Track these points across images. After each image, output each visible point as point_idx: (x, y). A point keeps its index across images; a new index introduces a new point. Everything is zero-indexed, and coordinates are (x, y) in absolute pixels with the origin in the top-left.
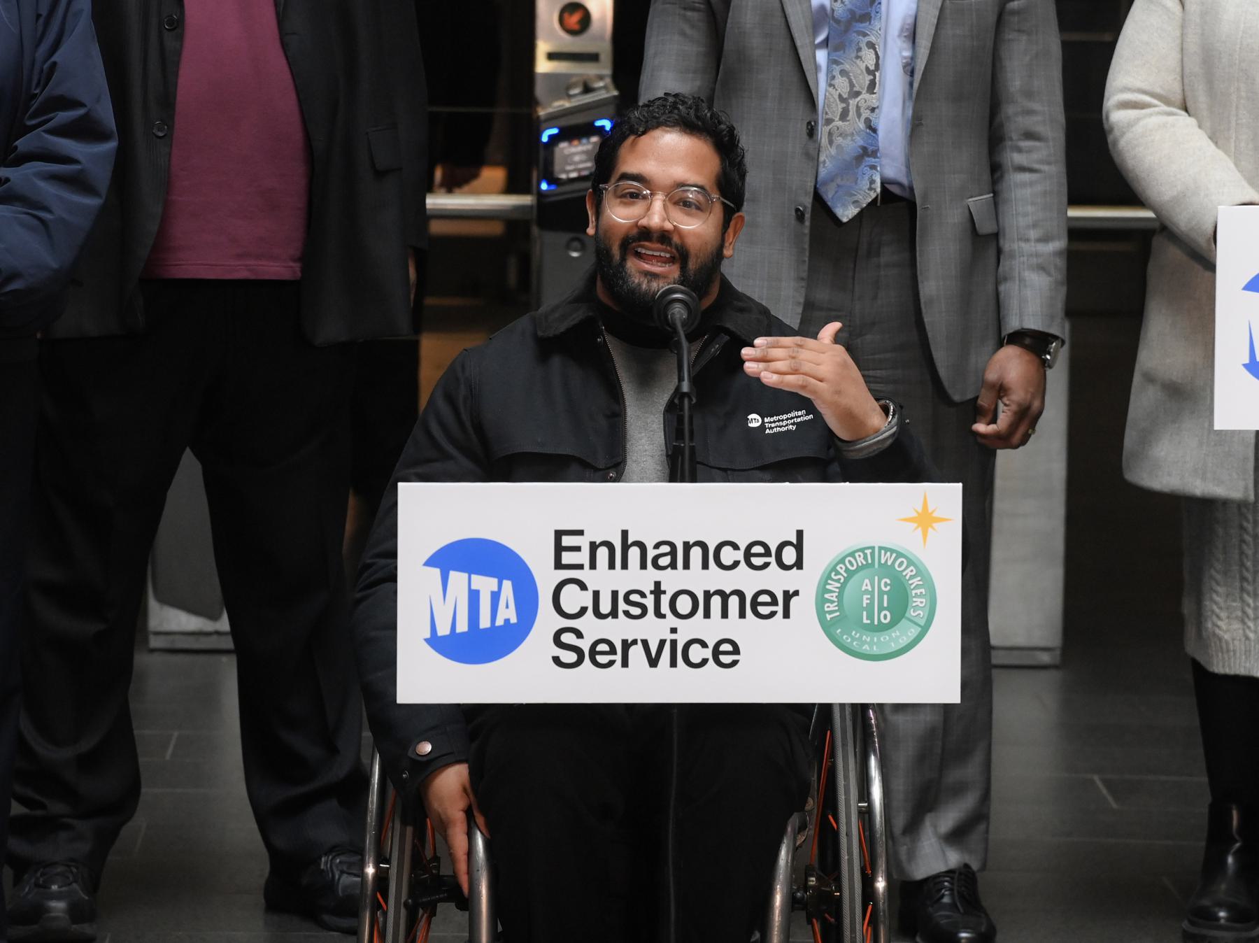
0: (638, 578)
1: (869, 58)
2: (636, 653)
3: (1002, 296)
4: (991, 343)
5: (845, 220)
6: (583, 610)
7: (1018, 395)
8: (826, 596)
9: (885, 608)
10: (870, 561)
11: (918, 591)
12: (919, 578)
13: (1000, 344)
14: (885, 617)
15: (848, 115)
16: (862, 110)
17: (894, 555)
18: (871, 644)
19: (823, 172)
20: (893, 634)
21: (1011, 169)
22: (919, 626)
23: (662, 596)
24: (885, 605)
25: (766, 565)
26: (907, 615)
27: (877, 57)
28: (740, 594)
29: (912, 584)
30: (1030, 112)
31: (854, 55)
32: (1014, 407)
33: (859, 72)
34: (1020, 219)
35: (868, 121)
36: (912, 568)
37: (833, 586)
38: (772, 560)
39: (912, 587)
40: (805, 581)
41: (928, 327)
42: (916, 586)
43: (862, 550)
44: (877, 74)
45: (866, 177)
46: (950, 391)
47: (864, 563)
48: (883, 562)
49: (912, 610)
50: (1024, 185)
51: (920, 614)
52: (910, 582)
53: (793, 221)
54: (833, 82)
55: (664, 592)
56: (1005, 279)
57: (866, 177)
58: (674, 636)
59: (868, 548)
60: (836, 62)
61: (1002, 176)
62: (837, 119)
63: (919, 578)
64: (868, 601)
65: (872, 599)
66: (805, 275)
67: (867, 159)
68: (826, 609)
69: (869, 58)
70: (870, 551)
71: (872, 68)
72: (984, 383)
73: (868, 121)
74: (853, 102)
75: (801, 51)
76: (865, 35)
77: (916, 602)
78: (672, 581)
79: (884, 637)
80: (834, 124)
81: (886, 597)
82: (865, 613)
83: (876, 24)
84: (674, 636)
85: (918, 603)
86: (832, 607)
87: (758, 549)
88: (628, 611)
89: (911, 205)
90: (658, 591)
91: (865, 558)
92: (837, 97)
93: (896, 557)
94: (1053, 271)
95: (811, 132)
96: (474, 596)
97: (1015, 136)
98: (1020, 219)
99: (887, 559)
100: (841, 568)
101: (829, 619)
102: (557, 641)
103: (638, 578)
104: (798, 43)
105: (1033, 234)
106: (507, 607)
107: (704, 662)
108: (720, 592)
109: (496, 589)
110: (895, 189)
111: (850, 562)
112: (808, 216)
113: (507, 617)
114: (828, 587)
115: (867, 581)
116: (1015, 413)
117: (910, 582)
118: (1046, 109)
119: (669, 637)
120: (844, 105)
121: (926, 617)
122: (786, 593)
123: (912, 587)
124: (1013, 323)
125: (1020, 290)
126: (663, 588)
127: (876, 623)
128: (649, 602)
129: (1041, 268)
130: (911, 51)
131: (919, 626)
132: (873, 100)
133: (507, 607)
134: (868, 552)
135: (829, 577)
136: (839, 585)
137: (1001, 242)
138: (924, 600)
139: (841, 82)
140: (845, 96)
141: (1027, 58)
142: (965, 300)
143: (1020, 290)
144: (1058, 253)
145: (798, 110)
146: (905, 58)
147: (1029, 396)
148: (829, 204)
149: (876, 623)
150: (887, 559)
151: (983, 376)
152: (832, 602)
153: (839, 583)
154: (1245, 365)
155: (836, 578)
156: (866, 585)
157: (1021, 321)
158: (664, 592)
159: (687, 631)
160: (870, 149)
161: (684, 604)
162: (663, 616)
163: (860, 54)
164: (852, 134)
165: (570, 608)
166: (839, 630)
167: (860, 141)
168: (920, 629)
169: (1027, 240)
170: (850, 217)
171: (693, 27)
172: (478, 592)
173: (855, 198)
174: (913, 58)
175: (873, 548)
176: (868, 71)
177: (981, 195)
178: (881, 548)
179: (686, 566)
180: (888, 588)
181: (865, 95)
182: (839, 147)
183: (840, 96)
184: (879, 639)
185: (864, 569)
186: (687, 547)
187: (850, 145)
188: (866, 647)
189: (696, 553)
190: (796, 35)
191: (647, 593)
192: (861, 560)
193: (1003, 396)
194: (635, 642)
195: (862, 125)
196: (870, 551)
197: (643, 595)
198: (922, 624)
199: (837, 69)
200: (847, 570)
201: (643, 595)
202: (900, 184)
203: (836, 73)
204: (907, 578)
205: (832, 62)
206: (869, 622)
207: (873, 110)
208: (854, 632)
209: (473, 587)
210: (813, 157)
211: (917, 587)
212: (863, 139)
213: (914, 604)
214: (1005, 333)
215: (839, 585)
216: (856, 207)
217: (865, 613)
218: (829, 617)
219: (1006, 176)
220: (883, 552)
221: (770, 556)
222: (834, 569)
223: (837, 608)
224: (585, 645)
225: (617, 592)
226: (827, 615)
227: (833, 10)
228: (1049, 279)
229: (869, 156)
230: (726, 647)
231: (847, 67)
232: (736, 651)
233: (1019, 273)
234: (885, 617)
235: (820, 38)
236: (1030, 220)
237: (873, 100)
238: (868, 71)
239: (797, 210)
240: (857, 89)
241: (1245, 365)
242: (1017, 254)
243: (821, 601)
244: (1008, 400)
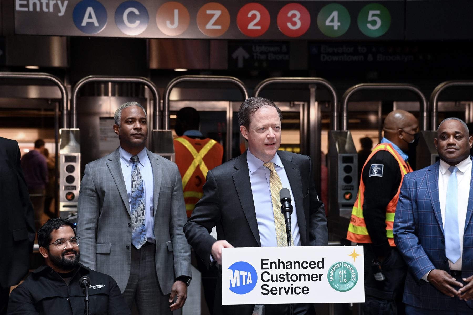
0: (282, 271)
1: (142, 207)
2: (283, 290)
3: (175, 267)
4: (173, 280)
5: (138, 249)
6: (269, 280)
7: (181, 294)
8: (330, 275)
11: (353, 274)
13: (175, 280)
15: (137, 222)
16: (141, 220)
17: (347, 264)
18: (342, 287)
19: (134, 235)
20: (347, 285)
21: (176, 235)
22: (354, 282)
24: (345, 277)
25: (315, 267)
26: (351, 280)
27: (144, 206)
28: (308, 275)
30: (179, 220)
31: (138, 206)
32: (180, 297)
33: (140, 210)
34: (179, 247)
35: (143, 223)
36: (351, 268)
37: (332, 272)
38: (316, 266)
39: (352, 272)
40: (325, 271)
41: (158, 276)
43: (339, 263)
44: (144, 211)
45: (143, 237)
46: (163, 292)
48: (344, 266)
50: (179, 238)
52: (351, 271)
53: (126, 249)
54: (133, 213)
55: (289, 275)
56: (176, 263)
57: (143, 237)
58: (292, 286)
59: (340, 263)
60: (134, 208)
61: (174, 237)
62: (135, 223)
66: (130, 263)
67: (143, 233)
68: (330, 279)
69: (142, 207)
71: (143, 209)
72: (172, 290)
73: (143, 223)
74: (138, 218)
75: (126, 205)
76: (141, 201)
78: (291, 272)
79: (345, 286)
80: (134, 224)
81: (345, 275)
82: (340, 279)
83: (143, 198)
84: (292, 286)
86: (332, 278)
87: (312, 263)
90: (287, 274)
91: (340, 265)
92: (134, 217)
94: (188, 260)
95: (130, 225)
96: (241, 277)
97: (176, 226)
98: (179, 247)
102: (262, 288)
103: (282, 271)
104: (125, 203)
105: (183, 251)
106: (250, 279)
107: (300, 293)
108: (303, 275)
109: (247, 275)
111: (336, 266)
112: (130, 247)
113: (250, 282)
114: (331, 273)
115: (340, 271)
116: (181, 298)
118: (184, 219)
119: (291, 286)
120: (136, 219)
121: (355, 280)
122: (320, 274)
124: (179, 274)
125: (180, 266)
126: (289, 274)
127: (343, 282)
128: (285, 277)
129: (185, 260)
130: (153, 204)
131: (354, 282)
133: (250, 279)
134: (340, 263)
136: (333, 272)
137: (174, 253)
138: (355, 276)
139: (135, 214)
140: (136, 217)
141: (178, 207)
142: (166, 268)
143: (180, 266)
144: (189, 256)
146: (151, 206)
147: (184, 294)
148: (134, 245)
149: (343, 282)
151: (172, 289)
152: (332, 277)
154: (229, 288)
155: (332, 270)
156: (340, 272)
157: (181, 273)
158: (289, 275)
159: (295, 284)
160: (144, 230)
161: (294, 278)
162: (289, 281)
163: (139, 206)
164: (139, 227)
166: (334, 284)
167: (141, 228)
168: (354, 283)
169: (181, 253)
170: (140, 248)
171: (93, 201)
173: (140, 243)
174: (154, 206)
175: (341, 263)
176: (142, 210)
177: (169, 241)
178: (343, 263)
179: (295, 268)
180: (346, 273)
181: (141, 216)
182: (136, 230)
183: (135, 217)
184: (344, 286)
186: (295, 263)
187: (139, 230)
188: (341, 288)
189: (297, 264)
190: (124, 201)
191: (285, 275)
192: (338, 266)
193: (177, 294)
194: (282, 288)
195: (141, 224)
197: (284, 276)
198: (355, 282)
199: (134, 210)
200: (335, 268)
201: (284, 276)
203: (134, 211)
204: (350, 270)
205: (133, 208)
206: (341, 282)
207: (144, 220)
208: (337, 285)
210: (130, 232)
212: (142, 228)
213: (352, 277)
214: (177, 277)
215: (333, 272)
216: (141, 245)
217: (340, 279)
218: (331, 280)
219: (175, 237)
220: (344, 264)
221: (316, 265)
222: (332, 268)
224: (269, 289)
225: (277, 275)
227: (132, 195)
228: (188, 262)
229: (143, 232)
230: (305, 289)
231: (136, 209)
232: (308, 290)
233: (180, 261)
235: (129, 201)
236: (182, 247)
237: (143, 217)
238: (142, 210)
239: (127, 246)
240: (139, 215)
241: (229, 288)
242: (179, 256)
243: (329, 277)
244: (179, 295)
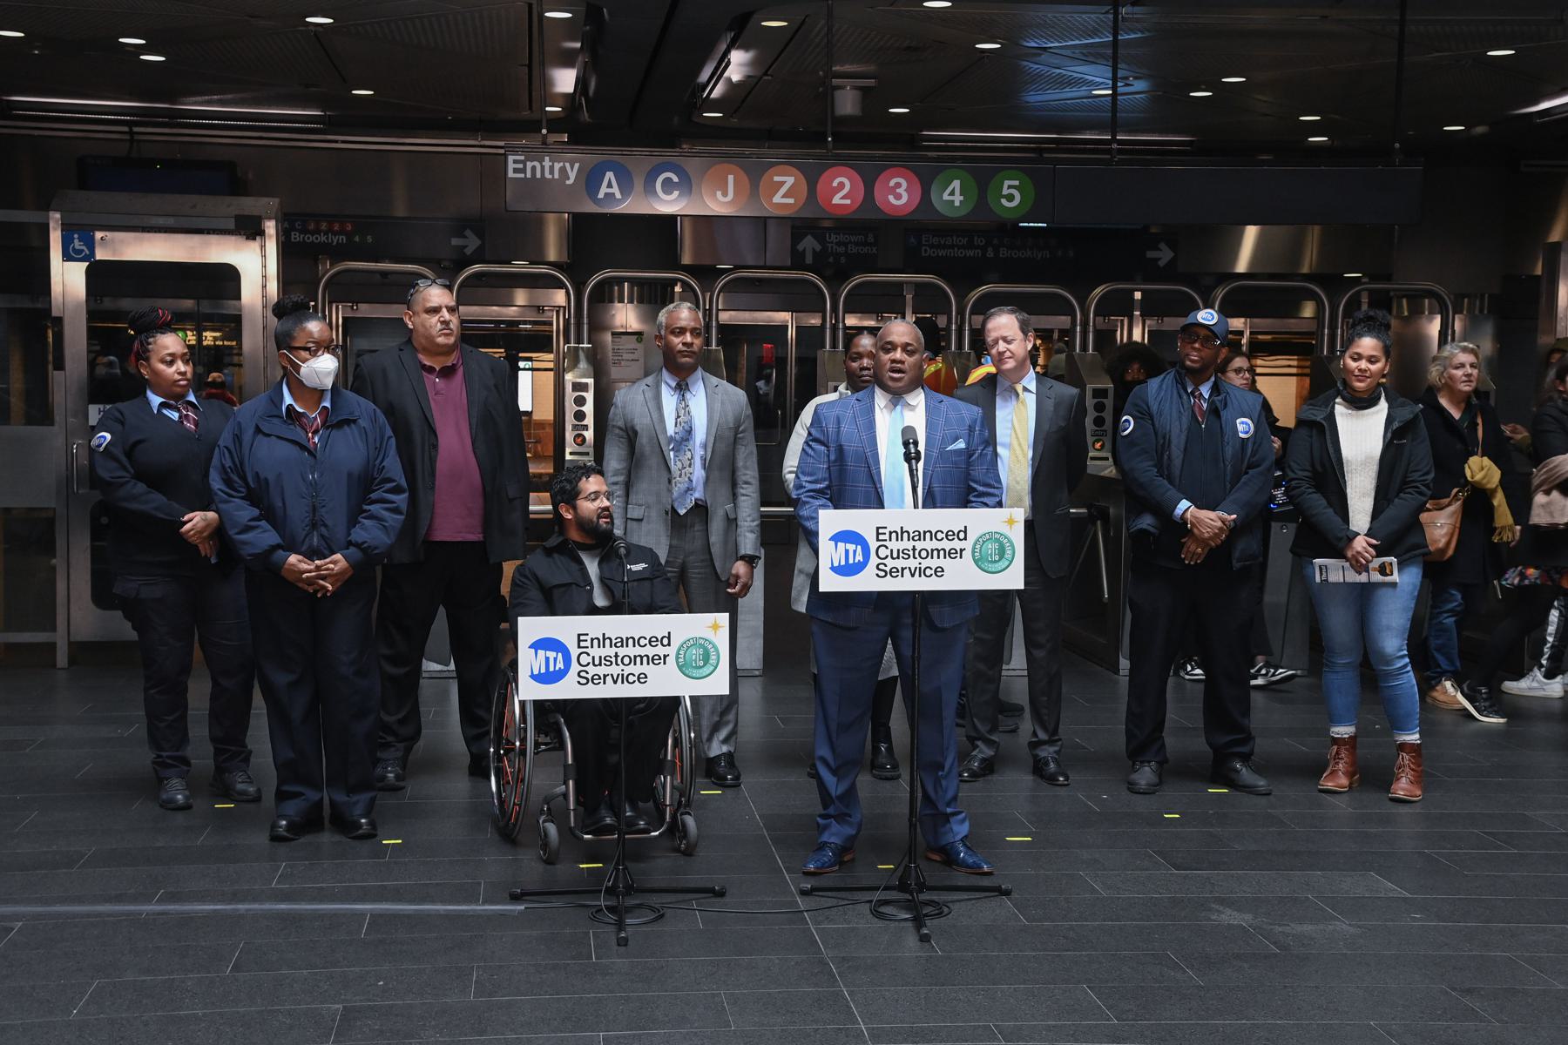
1: (689, 455)
19: (675, 494)
35: (689, 478)
69: (689, 455)
73: (689, 478)
89: (706, 508)
110: (700, 503)
132: (691, 470)
145: (665, 476)
187: (683, 487)
195: (687, 479)
199: (677, 459)
202: (701, 500)
210: (670, 491)
231: (680, 458)
235: (671, 447)
237: (691, 470)
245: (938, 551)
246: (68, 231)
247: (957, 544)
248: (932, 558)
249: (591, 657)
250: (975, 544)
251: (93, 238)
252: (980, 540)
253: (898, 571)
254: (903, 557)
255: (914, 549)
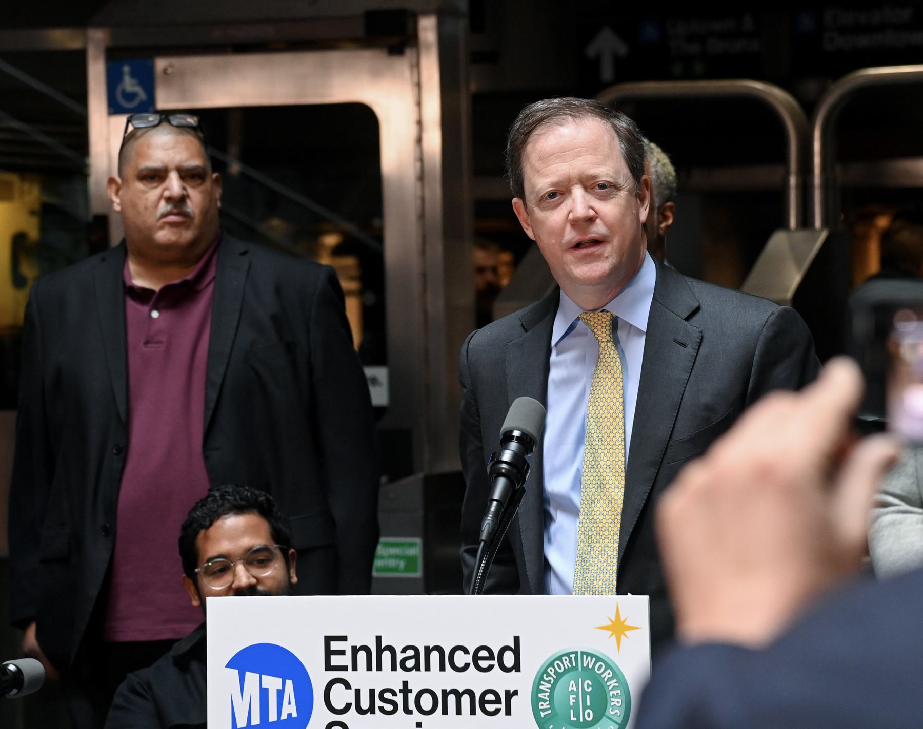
0: (390, 679)
6: (348, 706)
8: (540, 695)
9: (589, 706)
10: (574, 665)
11: (615, 692)
12: (615, 681)
14: (589, 715)
17: (594, 659)
23: (409, 694)
24: (588, 704)
25: (491, 668)
26: (606, 713)
29: (610, 685)
36: (609, 671)
37: (545, 686)
38: (495, 663)
39: (610, 688)
42: (613, 688)
43: (568, 655)
47: (570, 666)
48: (585, 665)
49: (611, 709)
51: (617, 713)
52: (608, 684)
55: (411, 691)
63: (615, 681)
64: (574, 701)
65: (577, 699)
68: (540, 707)
70: (574, 655)
77: (613, 702)
78: (417, 681)
81: (588, 697)
82: (572, 711)
85: (616, 703)
86: (545, 705)
87: (483, 653)
88: (383, 707)
90: (406, 690)
91: (570, 662)
93: (595, 661)
99: (588, 663)
100: (551, 671)
101: (543, 716)
103: (390, 679)
108: (454, 691)
111: (558, 664)
114: (541, 687)
115: (572, 682)
117: (608, 684)
123: (610, 688)
126: (409, 688)
127: (581, 720)
128: (399, 699)
134: (573, 656)
135: (542, 679)
136: (550, 686)
149: (581, 720)
150: (588, 663)
152: (545, 701)
153: (550, 684)
156: (572, 686)
158: (411, 691)
161: (427, 702)
162: (410, 712)
165: (338, 704)
172: (267, 689)
175: (576, 653)
178: (583, 653)
179: (428, 668)
180: (590, 688)
185: (573, 671)
186: (428, 650)
189: (435, 656)
191: (398, 692)
192: (567, 663)
196: (574, 655)
197: (394, 694)
200: (556, 672)
201: (394, 694)
204: (606, 680)
206: (575, 719)
209: (263, 686)
211: (614, 688)
213: (612, 704)
215: (550, 686)
217: (572, 711)
218: (542, 714)
220: (585, 656)
222: (545, 671)
223: (549, 707)
225: (374, 690)
226: (541, 712)
234: (589, 715)
243: (536, 700)
245: (458, 695)
246: (113, 56)
247: (498, 681)
248: (445, 712)
249: (352, 693)
250: (539, 680)
251: (151, 70)
252: (551, 671)
253: (498, 701)
254: (382, 709)
255: (406, 690)
